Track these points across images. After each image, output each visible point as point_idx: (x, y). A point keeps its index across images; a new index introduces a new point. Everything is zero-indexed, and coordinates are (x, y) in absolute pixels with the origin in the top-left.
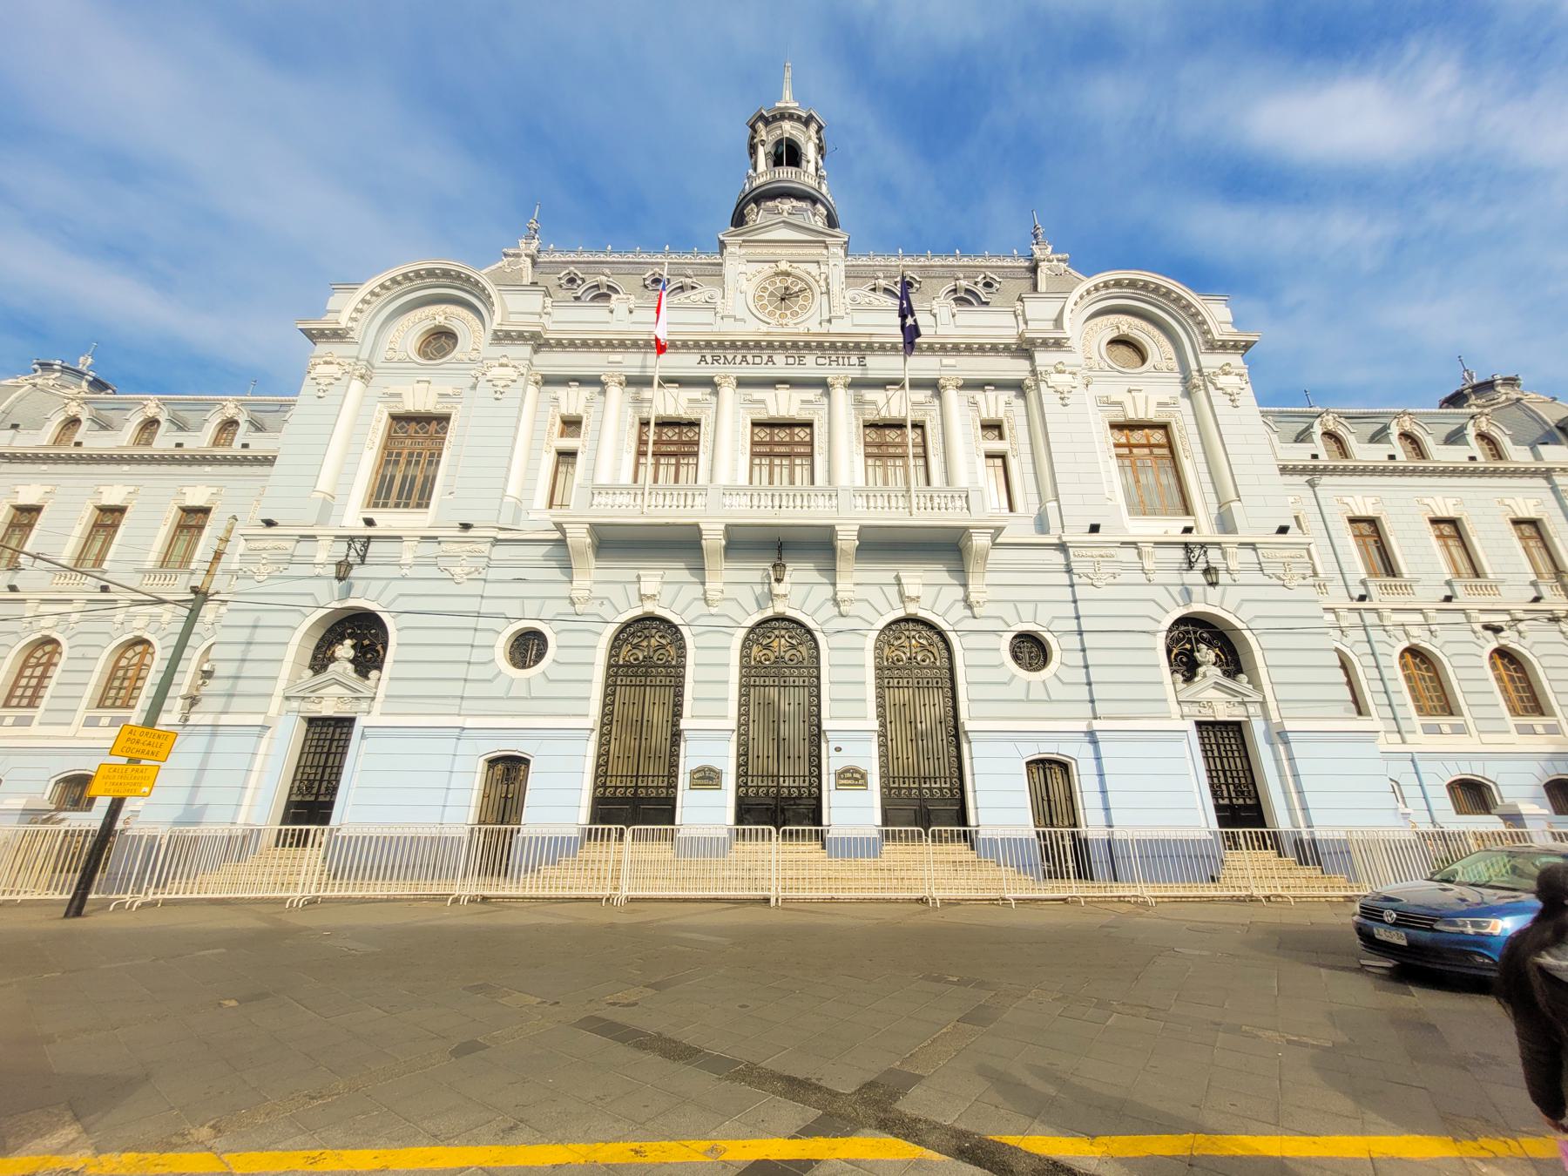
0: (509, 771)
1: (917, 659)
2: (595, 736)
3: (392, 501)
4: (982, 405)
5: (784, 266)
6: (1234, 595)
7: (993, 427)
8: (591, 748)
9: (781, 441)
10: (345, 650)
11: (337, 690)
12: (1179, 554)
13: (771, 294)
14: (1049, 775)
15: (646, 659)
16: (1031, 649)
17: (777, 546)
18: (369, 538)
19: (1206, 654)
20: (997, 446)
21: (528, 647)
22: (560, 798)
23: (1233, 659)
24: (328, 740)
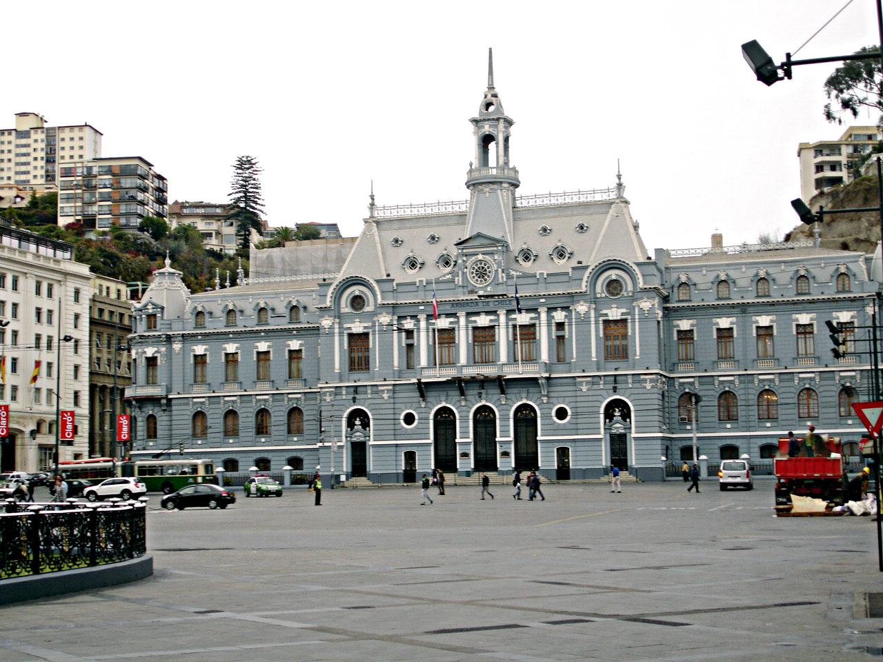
0: (410, 457)
1: (525, 420)
2: (433, 445)
3: (356, 367)
4: (556, 318)
5: (480, 257)
6: (629, 392)
7: (560, 326)
8: (432, 448)
9: (484, 336)
10: (358, 422)
11: (358, 434)
12: (613, 378)
13: (477, 271)
14: (563, 453)
15: (445, 422)
16: (561, 414)
17: (482, 383)
18: (357, 386)
19: (617, 413)
20: (560, 333)
21: (409, 419)
22: (426, 463)
23: (626, 415)
24: (359, 450)
